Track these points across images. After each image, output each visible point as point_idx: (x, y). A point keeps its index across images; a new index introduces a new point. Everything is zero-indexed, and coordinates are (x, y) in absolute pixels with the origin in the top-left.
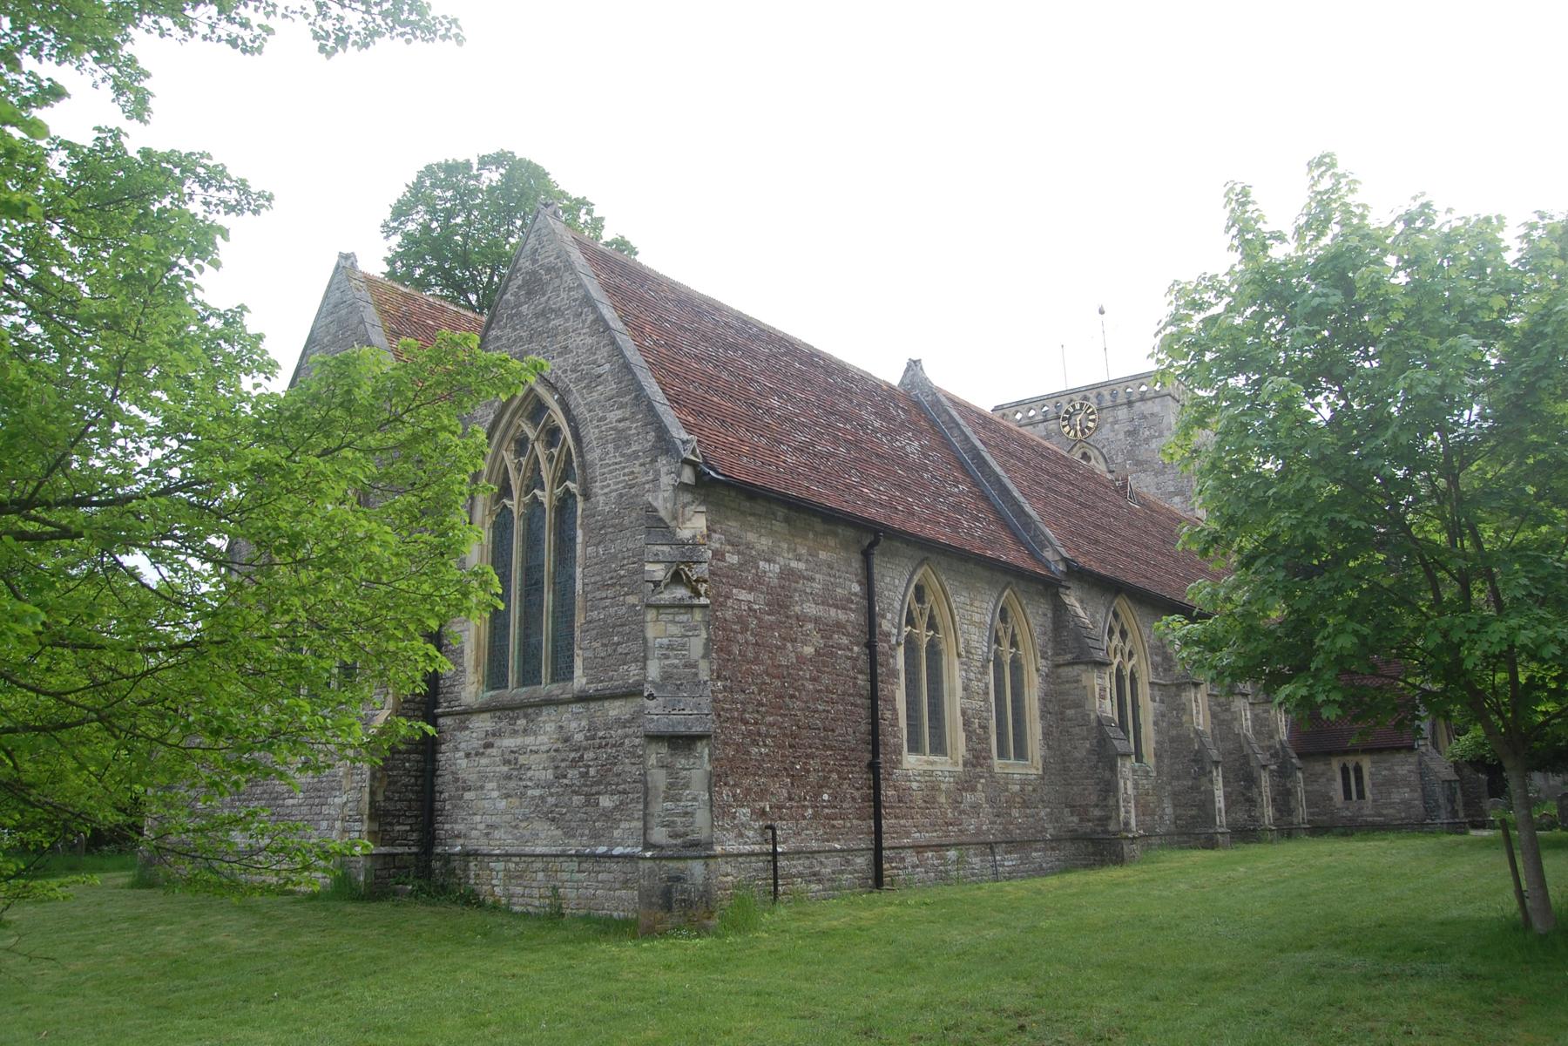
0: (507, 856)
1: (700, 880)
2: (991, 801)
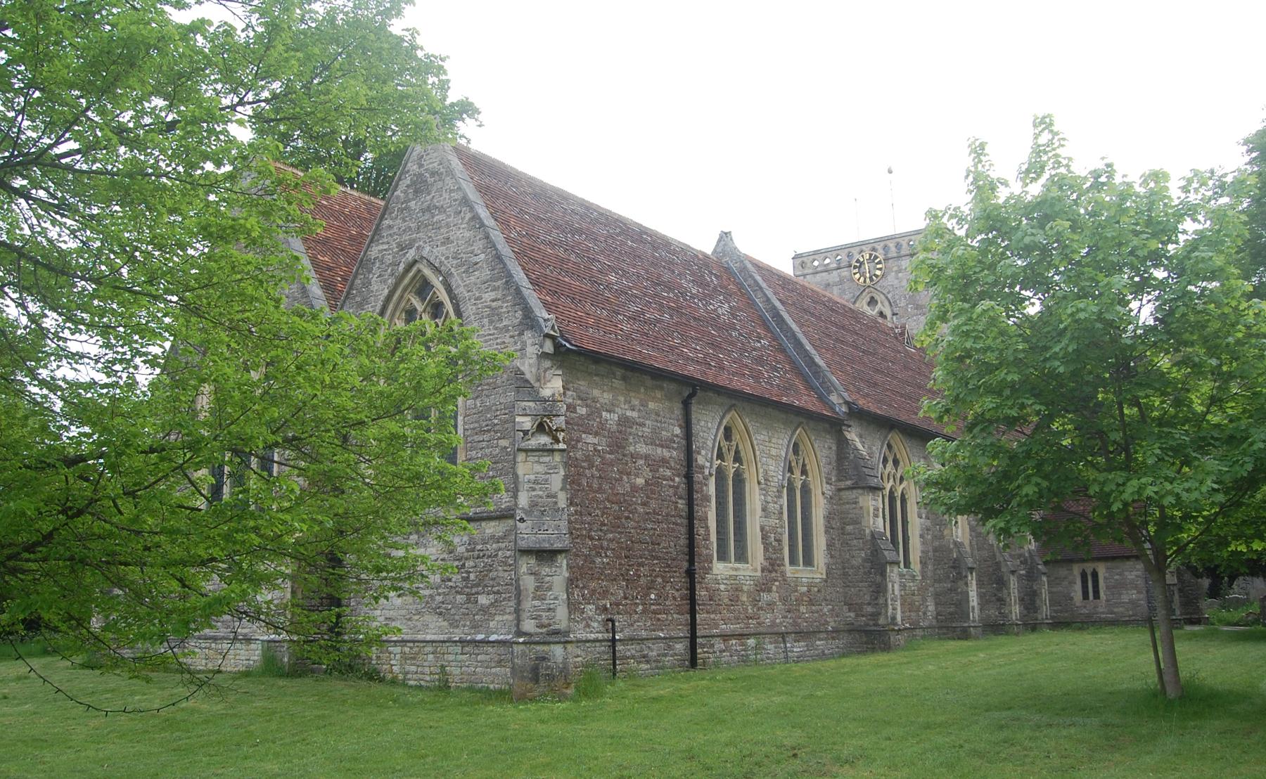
1: (560, 660)
2: (784, 600)
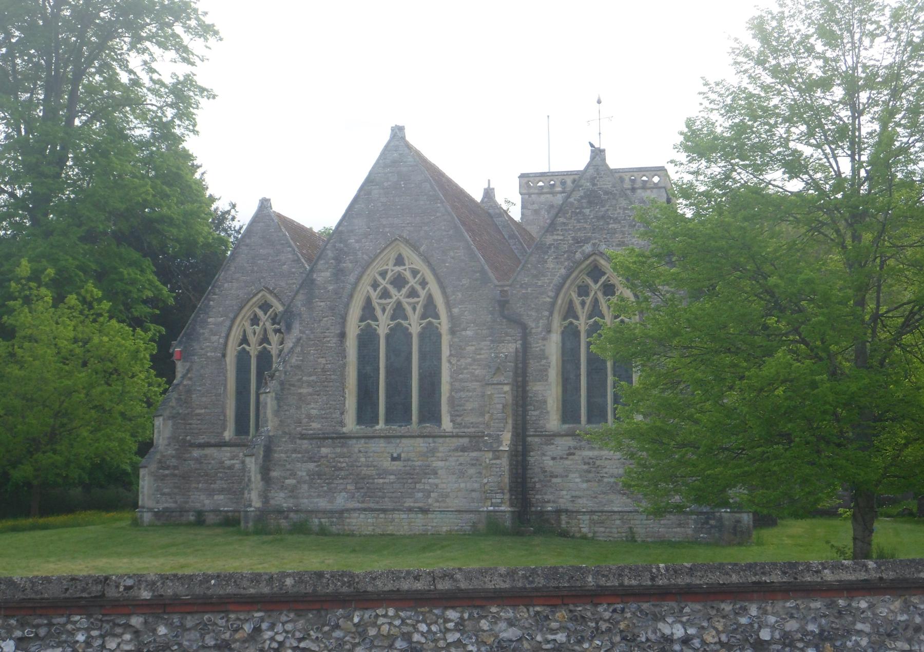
0: (592, 512)
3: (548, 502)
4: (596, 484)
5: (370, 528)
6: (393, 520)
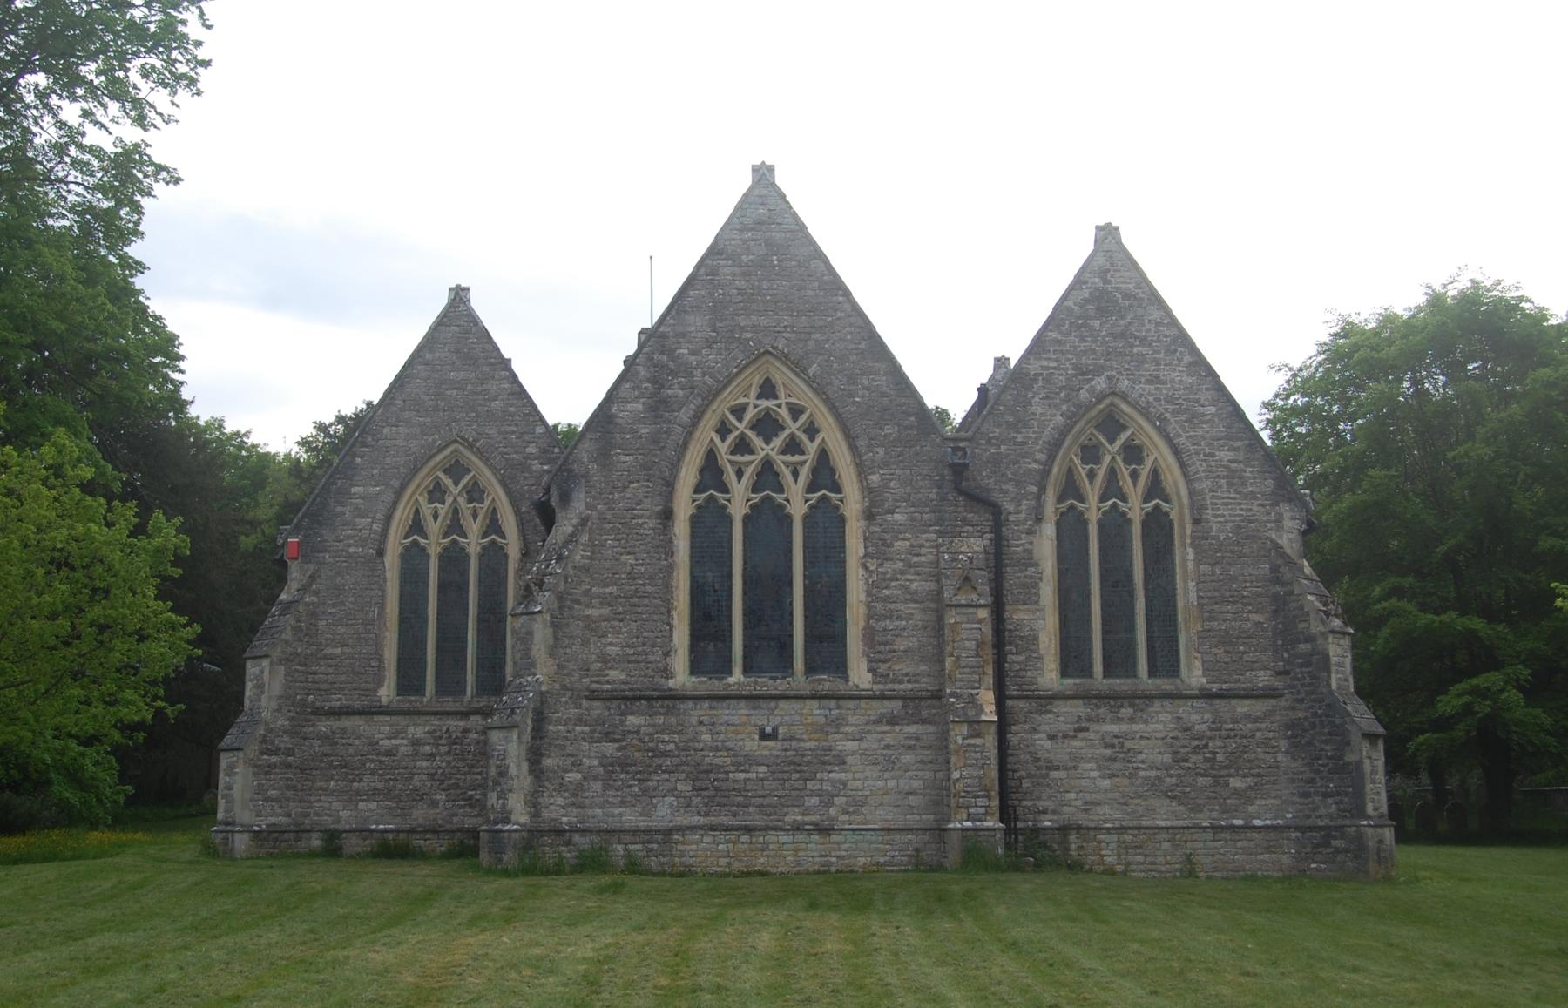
0: (1123, 829)
3: (1045, 812)
4: (1126, 781)
5: (723, 861)
6: (766, 845)
